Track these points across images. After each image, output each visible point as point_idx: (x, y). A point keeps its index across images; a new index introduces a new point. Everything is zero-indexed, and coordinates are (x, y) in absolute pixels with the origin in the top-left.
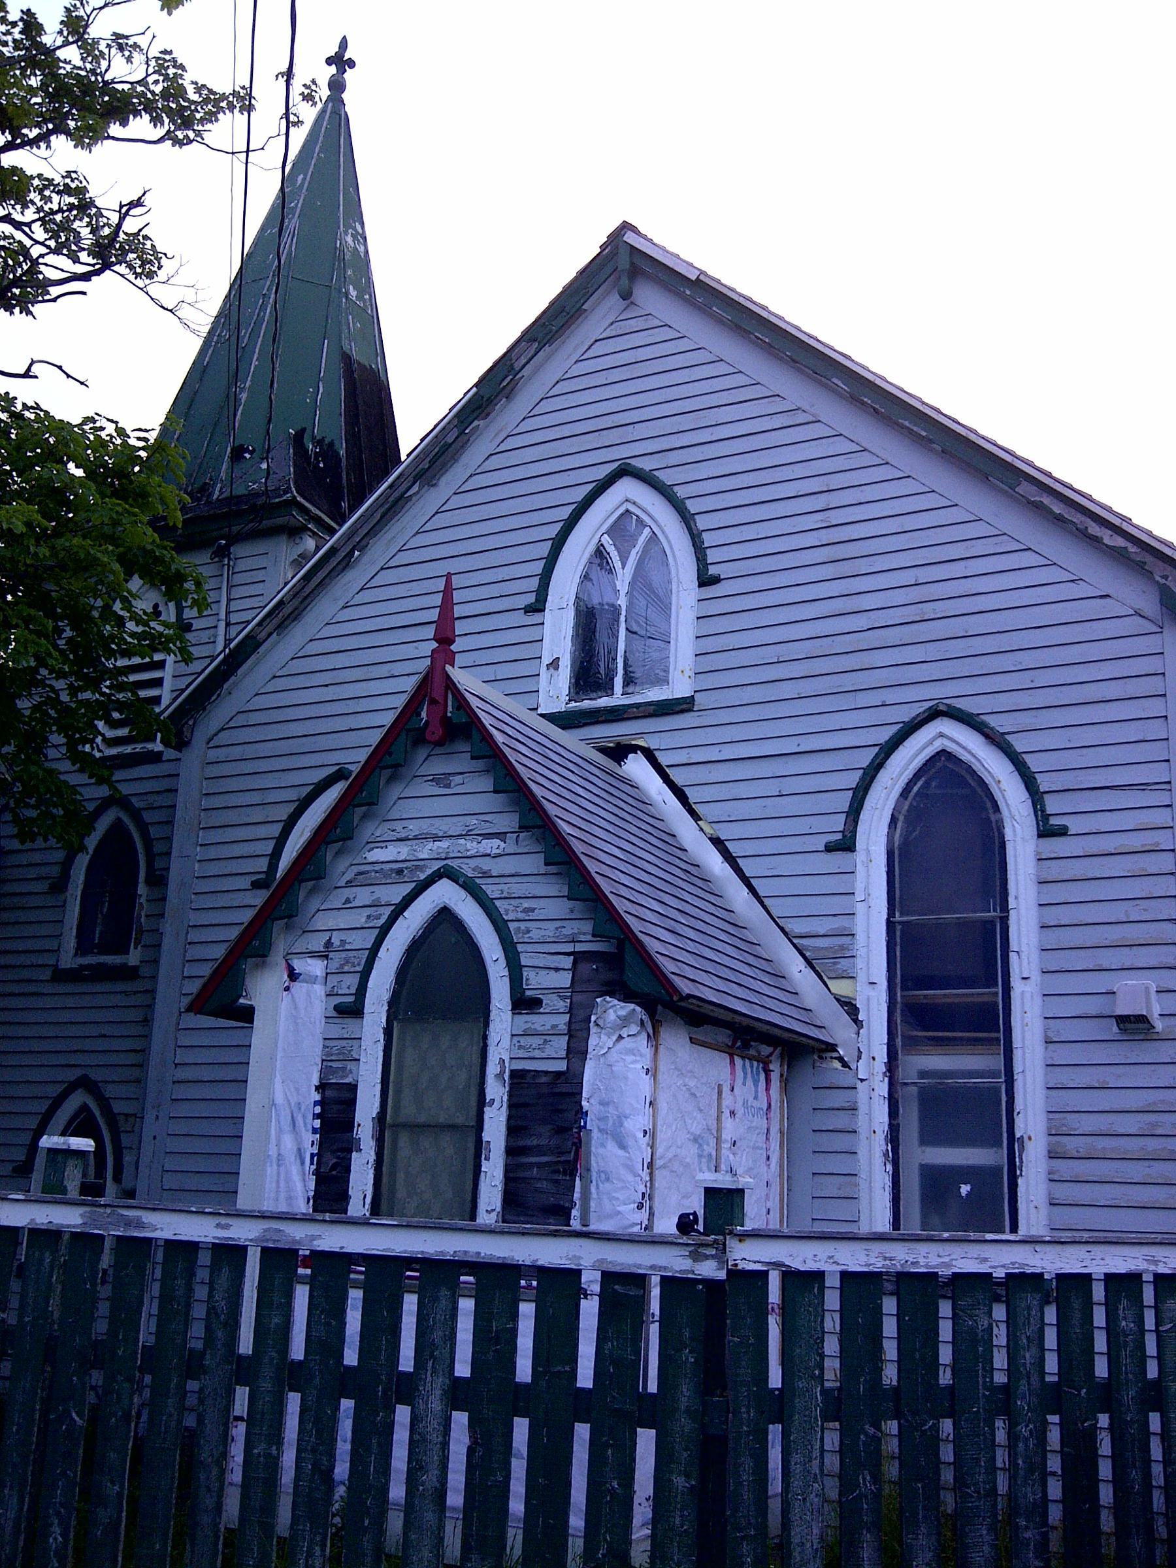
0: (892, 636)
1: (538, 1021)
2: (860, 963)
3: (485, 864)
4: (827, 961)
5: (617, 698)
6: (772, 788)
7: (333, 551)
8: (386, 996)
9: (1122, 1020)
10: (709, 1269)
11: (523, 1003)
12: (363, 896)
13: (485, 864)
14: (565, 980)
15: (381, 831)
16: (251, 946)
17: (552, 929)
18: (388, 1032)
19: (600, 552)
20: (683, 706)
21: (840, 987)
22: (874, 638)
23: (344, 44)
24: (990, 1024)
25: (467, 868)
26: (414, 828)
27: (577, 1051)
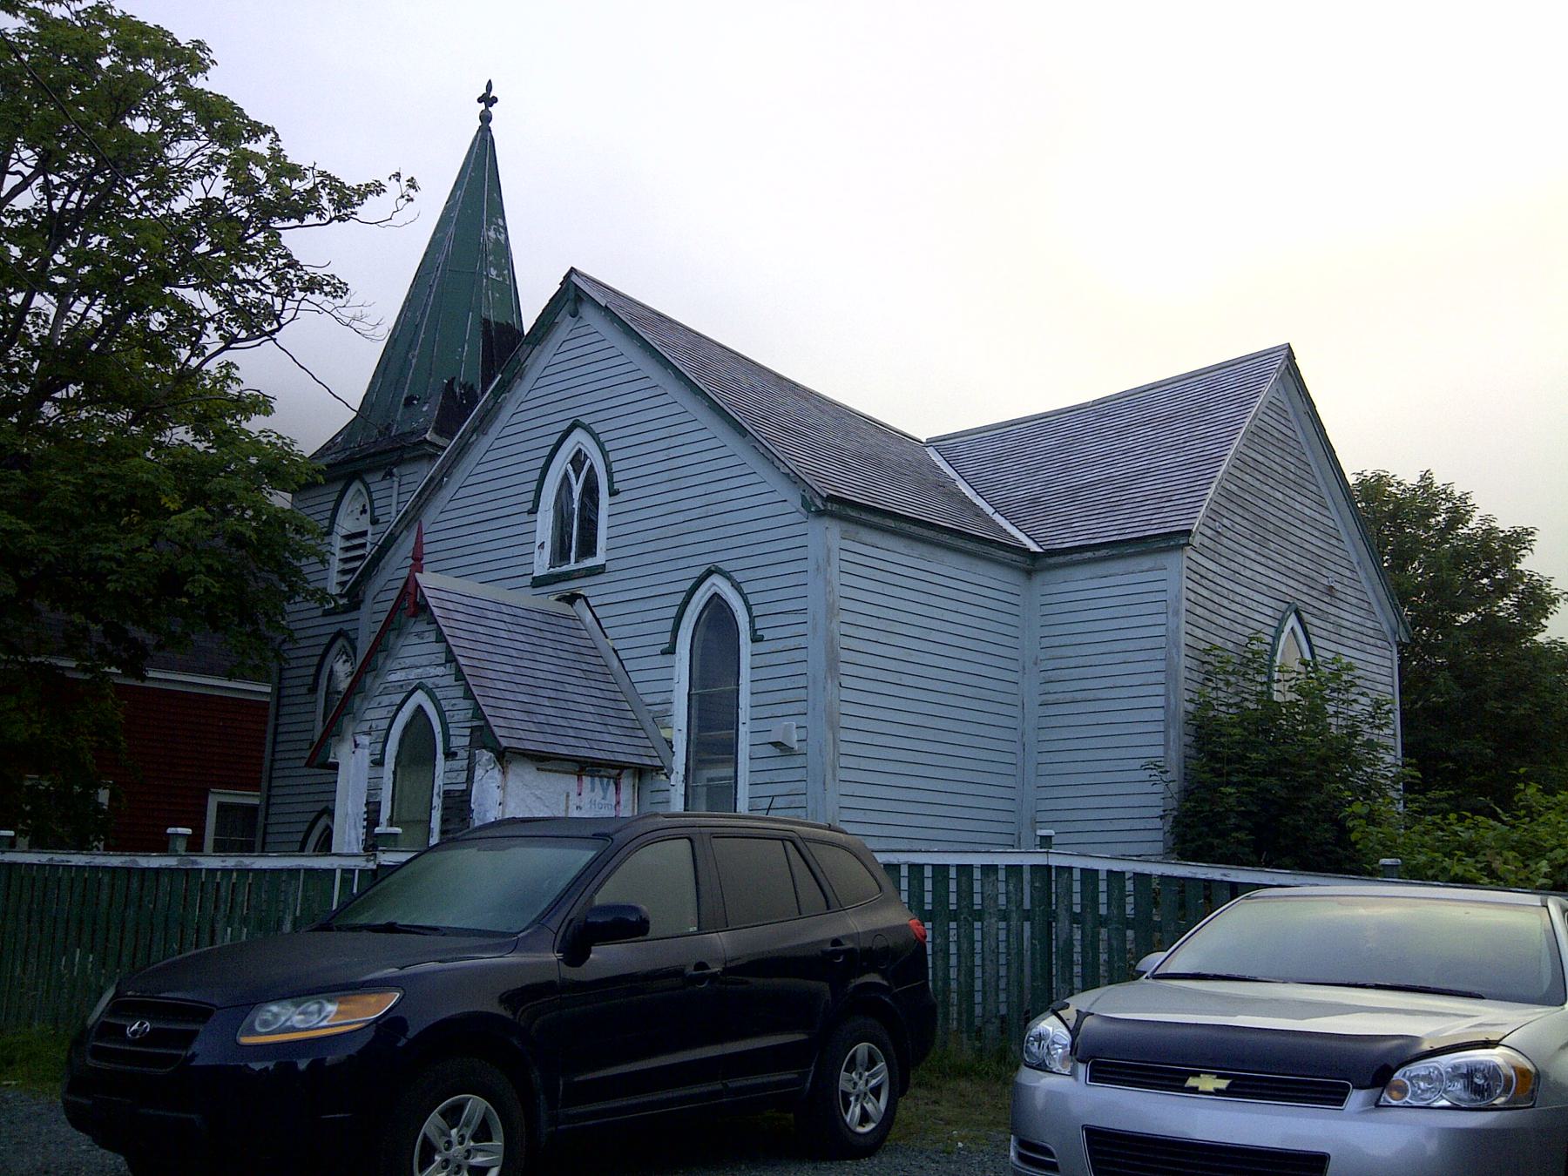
0: (694, 526)
1: (456, 764)
2: (675, 718)
3: (437, 681)
4: (662, 717)
6: (638, 618)
7: (432, 479)
9: (775, 744)
10: (372, 866)
11: (450, 755)
12: (386, 700)
13: (437, 681)
14: (466, 741)
15: (395, 665)
16: (333, 730)
17: (460, 713)
18: (395, 773)
19: (566, 477)
21: (665, 733)
22: (685, 527)
23: (489, 86)
24: (729, 750)
25: (429, 683)
26: (408, 662)
27: (470, 779)
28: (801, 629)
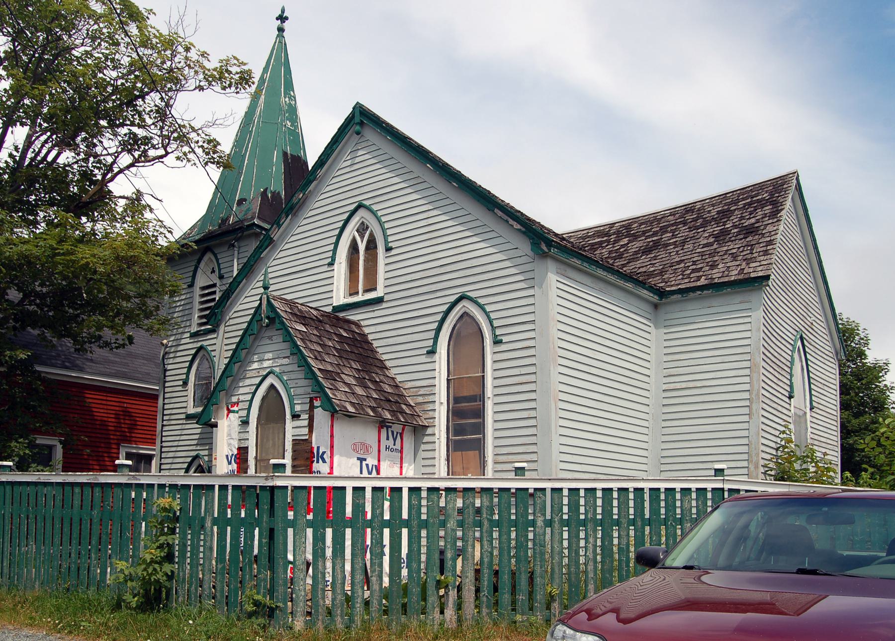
5: (360, 298)
8: (256, 416)
18: (257, 428)
20: (380, 300)
23: (283, 11)
28: (531, 335)
